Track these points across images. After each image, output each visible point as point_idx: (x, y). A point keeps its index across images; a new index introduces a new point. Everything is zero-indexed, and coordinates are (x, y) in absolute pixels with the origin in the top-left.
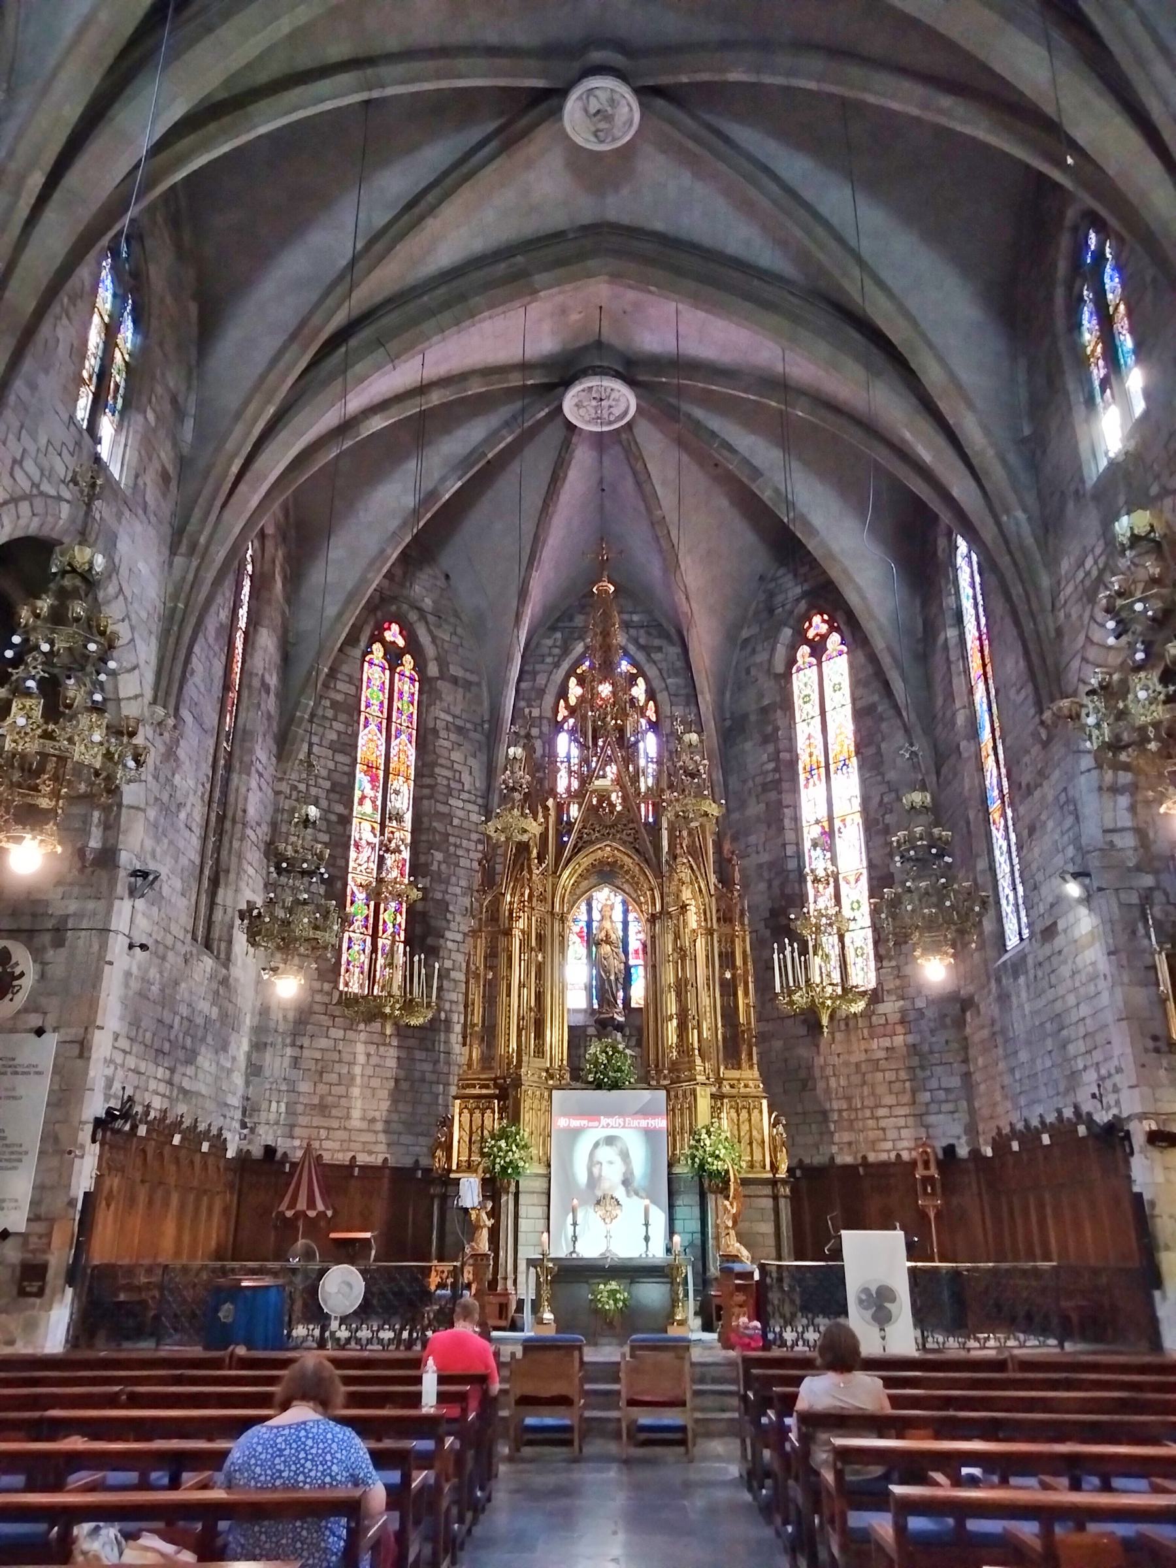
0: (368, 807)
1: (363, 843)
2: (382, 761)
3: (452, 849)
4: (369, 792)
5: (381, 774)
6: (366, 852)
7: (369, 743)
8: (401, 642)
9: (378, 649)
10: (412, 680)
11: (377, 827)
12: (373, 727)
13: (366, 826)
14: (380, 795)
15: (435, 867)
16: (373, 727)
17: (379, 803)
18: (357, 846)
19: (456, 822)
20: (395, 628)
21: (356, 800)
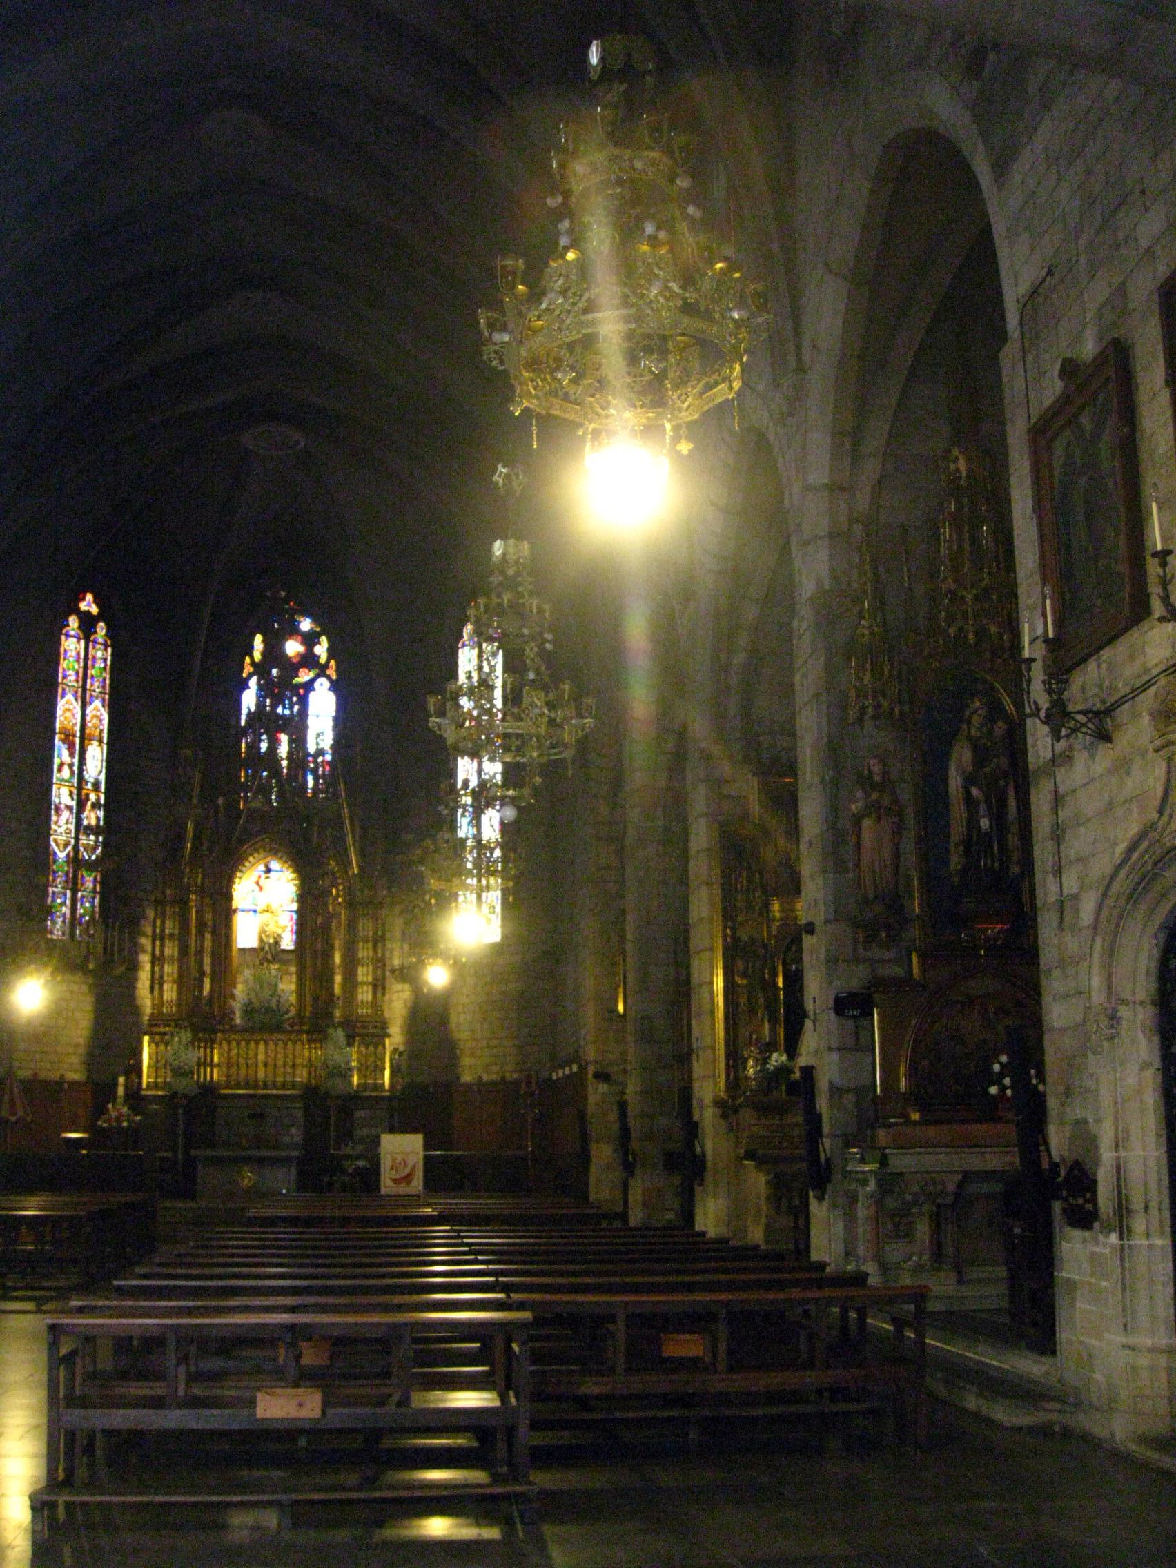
0: (66, 773)
1: (62, 806)
2: (78, 728)
4: (66, 757)
5: (77, 741)
6: (66, 815)
7: (67, 710)
8: (94, 610)
9: (73, 622)
10: (106, 646)
11: (75, 791)
12: (69, 697)
13: (65, 791)
14: (76, 761)
16: (69, 697)
17: (75, 768)
18: (57, 809)
20: (89, 597)
21: (55, 767)
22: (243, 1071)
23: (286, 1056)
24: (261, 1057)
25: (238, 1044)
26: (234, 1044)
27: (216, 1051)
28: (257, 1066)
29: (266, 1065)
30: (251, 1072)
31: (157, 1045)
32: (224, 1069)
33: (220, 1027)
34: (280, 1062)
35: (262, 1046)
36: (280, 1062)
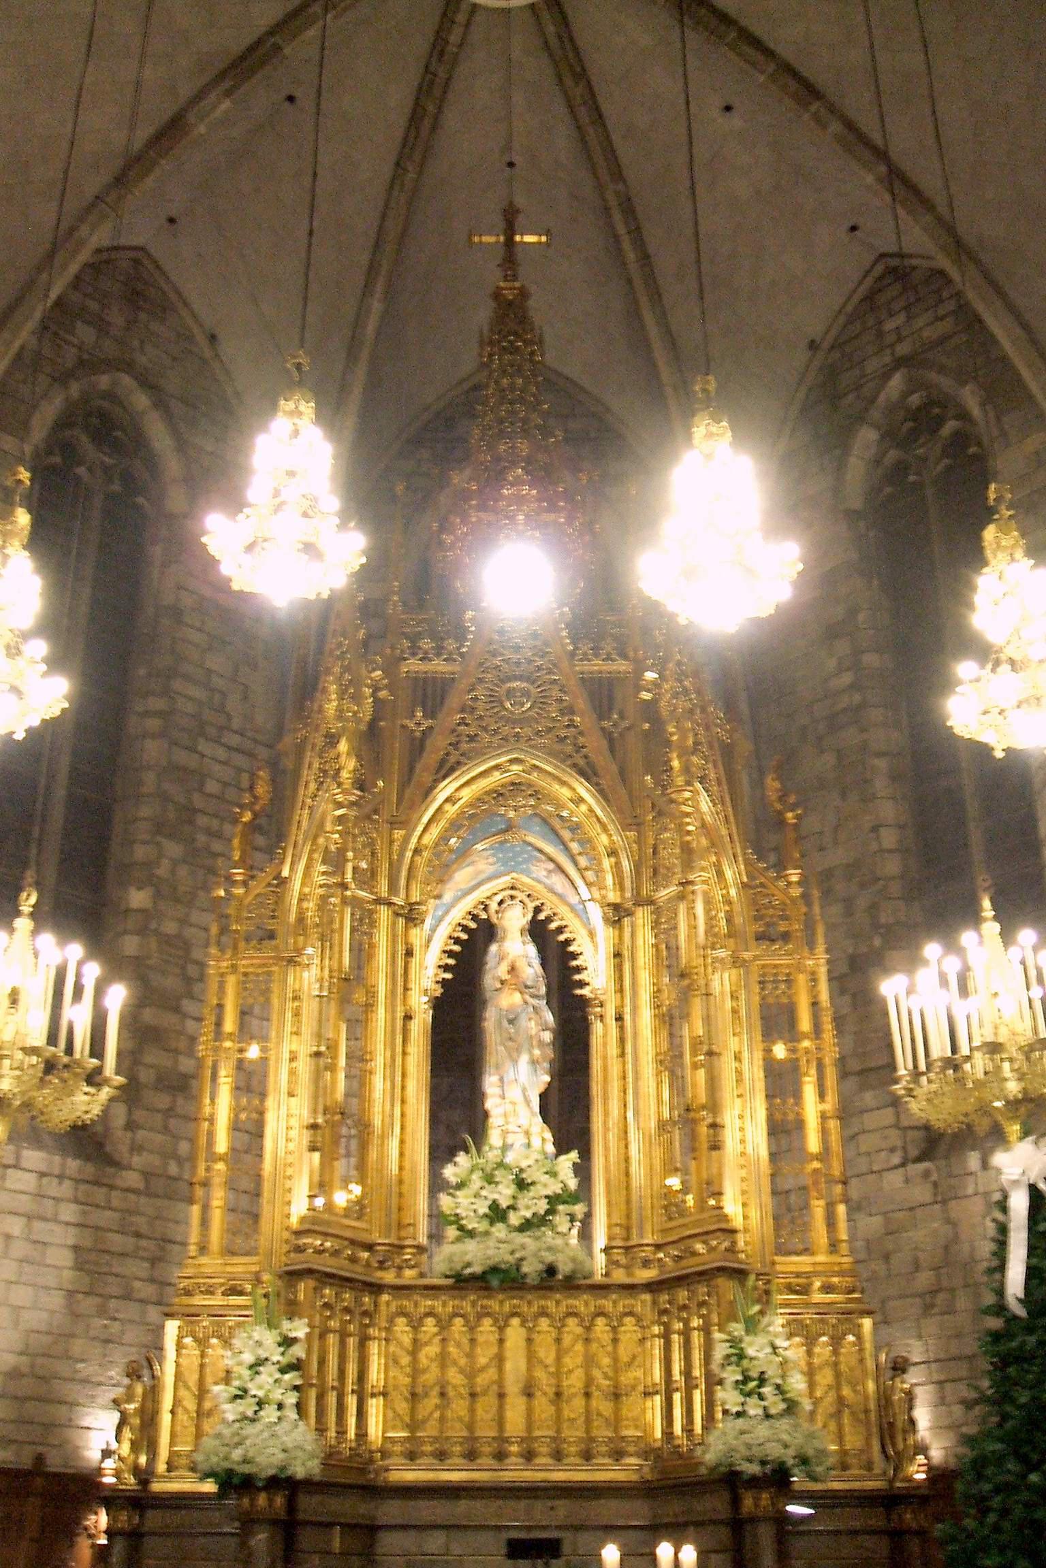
3: (202, 839)
15: (162, 871)
19: (212, 787)
22: (459, 1407)
23: (589, 1362)
24: (515, 1365)
25: (444, 1325)
26: (430, 1325)
27: (374, 1348)
28: (501, 1396)
29: (528, 1393)
30: (485, 1409)
31: (202, 1343)
32: (402, 1407)
33: (389, 1277)
34: (574, 1382)
35: (515, 1333)
36: (574, 1382)
